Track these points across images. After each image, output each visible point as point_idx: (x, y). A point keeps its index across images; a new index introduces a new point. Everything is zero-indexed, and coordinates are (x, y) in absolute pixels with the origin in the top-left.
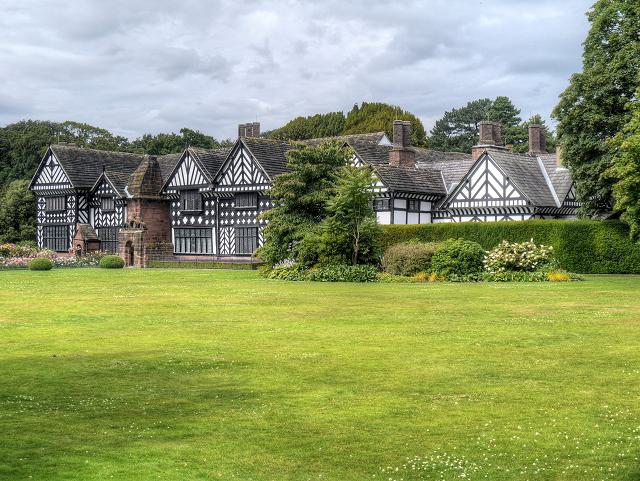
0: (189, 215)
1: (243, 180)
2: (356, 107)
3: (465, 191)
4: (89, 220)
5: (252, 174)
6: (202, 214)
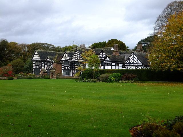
0: (66, 67)
1: (77, 59)
2: (109, 40)
3: (128, 61)
4: (44, 67)
5: (79, 57)
6: (69, 66)
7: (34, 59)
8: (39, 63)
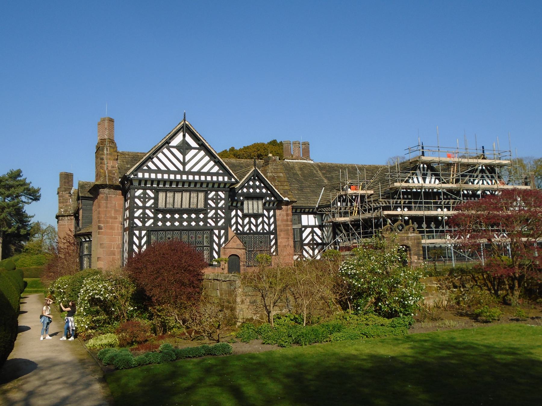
7: (159, 171)
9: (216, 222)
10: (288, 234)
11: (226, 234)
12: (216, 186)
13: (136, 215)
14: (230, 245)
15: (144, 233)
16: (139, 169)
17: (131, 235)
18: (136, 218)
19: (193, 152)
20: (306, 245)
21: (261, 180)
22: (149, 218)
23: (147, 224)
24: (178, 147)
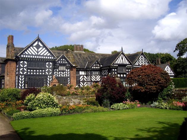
5: (145, 63)
6: (126, 74)
7: (29, 55)
8: (46, 65)
9: (49, 73)
10: (74, 78)
11: (52, 77)
12: (49, 61)
13: (21, 70)
14: (54, 81)
15: (23, 76)
16: (22, 54)
17: (19, 77)
18: (21, 71)
19: (41, 48)
20: (81, 82)
21: (65, 59)
22: (25, 71)
23: (24, 73)
24: (36, 46)
